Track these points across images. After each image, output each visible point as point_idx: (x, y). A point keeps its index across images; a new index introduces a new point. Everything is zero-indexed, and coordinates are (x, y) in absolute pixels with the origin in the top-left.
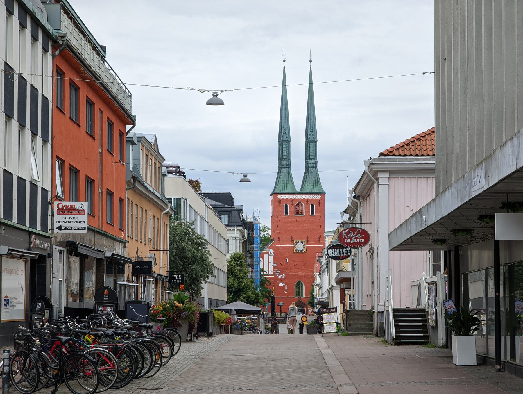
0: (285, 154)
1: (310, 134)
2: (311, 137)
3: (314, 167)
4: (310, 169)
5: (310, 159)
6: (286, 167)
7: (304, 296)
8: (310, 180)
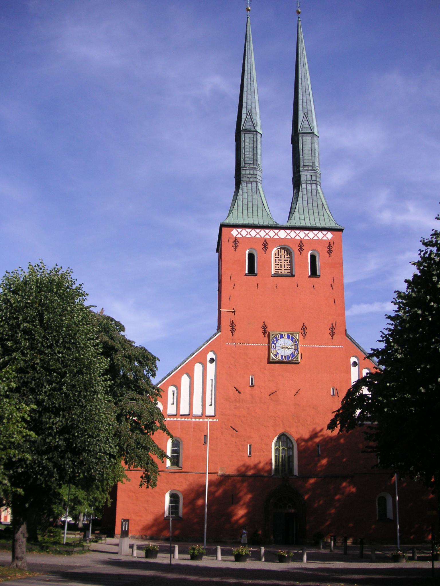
2: (305, 126)
3: (314, 182)
4: (304, 186)
6: (251, 180)
7: (296, 472)
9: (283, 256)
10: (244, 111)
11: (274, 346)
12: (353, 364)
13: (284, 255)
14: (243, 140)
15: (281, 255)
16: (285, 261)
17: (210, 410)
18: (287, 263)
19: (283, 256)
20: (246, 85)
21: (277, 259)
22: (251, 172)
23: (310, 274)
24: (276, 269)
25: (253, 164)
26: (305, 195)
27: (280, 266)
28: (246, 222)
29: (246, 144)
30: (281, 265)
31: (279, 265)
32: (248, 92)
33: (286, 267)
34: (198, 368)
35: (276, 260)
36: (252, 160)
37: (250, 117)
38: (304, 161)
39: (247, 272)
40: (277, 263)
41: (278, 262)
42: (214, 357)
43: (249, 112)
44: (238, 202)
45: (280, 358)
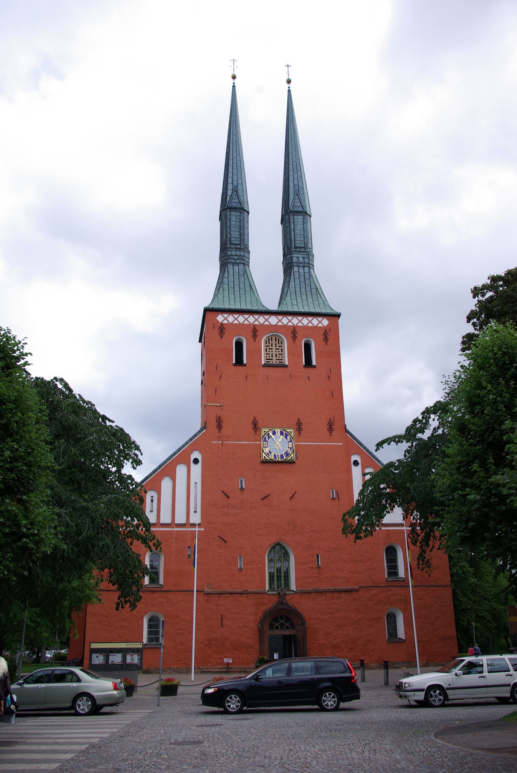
0: (235, 234)
1: (294, 199)
2: (296, 204)
4: (296, 269)
5: (296, 247)
6: (238, 261)
7: (293, 586)
8: (298, 289)
9: (274, 345)
10: (230, 187)
11: (266, 444)
12: (353, 463)
13: (276, 344)
14: (229, 218)
15: (272, 344)
16: (276, 350)
17: (196, 518)
18: (279, 352)
19: (274, 345)
20: (232, 159)
21: (268, 348)
22: (238, 253)
23: (304, 364)
24: (267, 359)
25: (240, 244)
26: (297, 278)
27: (270, 355)
28: (233, 307)
29: (232, 223)
30: (272, 354)
31: (269, 354)
32: (234, 166)
33: (278, 356)
34: (181, 470)
35: (266, 349)
36: (239, 240)
37: (235, 193)
38: (296, 243)
39: (234, 362)
40: (268, 352)
41: (269, 351)
42: (200, 458)
43: (234, 187)
44: (224, 285)
45: (273, 458)
